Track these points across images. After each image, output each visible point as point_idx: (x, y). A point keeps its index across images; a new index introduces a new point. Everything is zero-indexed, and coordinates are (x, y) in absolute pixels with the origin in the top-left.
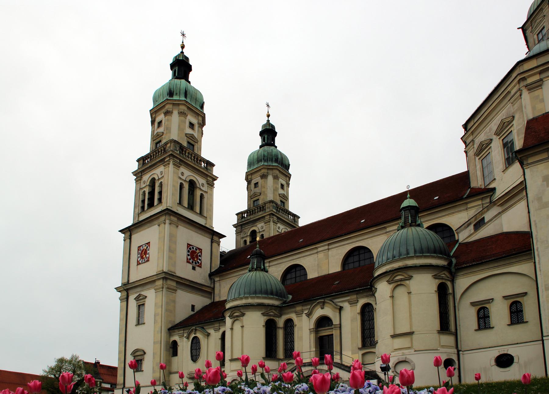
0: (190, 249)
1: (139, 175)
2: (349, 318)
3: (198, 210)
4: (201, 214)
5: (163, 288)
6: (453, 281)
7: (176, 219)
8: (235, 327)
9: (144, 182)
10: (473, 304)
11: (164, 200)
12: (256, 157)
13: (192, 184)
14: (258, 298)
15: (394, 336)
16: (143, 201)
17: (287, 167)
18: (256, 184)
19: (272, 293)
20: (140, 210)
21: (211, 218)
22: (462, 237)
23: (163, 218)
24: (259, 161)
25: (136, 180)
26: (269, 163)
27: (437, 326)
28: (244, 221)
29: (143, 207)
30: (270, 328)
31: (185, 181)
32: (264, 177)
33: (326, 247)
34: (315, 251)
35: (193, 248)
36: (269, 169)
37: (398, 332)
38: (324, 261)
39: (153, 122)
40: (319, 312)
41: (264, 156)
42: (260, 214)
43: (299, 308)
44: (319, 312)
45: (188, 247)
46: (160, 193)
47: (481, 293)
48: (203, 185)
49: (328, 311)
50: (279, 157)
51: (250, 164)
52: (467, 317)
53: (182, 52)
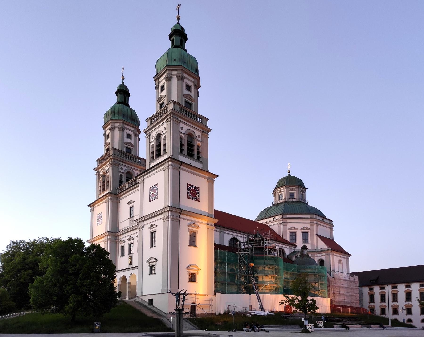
0: (190, 188)
3: (196, 157)
5: (168, 218)
11: (168, 151)
13: (190, 136)
23: (167, 165)
31: (184, 134)
35: (192, 187)
39: (157, 88)
45: (188, 187)
46: (165, 145)
53: (178, 23)
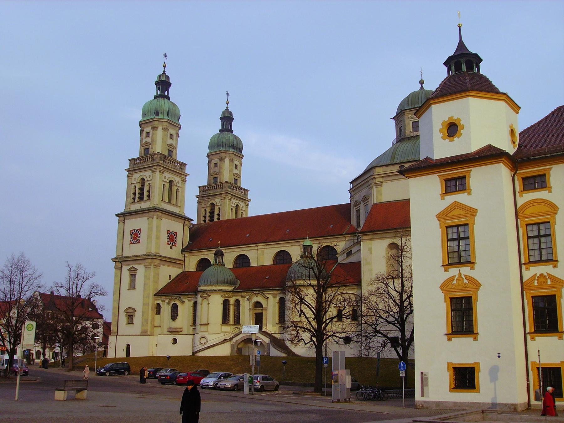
2: (271, 304)
4: (176, 205)
7: (160, 214)
8: (204, 304)
9: (135, 179)
12: (216, 141)
14: (219, 286)
17: (240, 150)
18: (216, 164)
19: (227, 283)
20: (132, 201)
21: (183, 207)
22: (341, 259)
24: (219, 145)
25: (129, 176)
26: (226, 146)
28: (205, 194)
30: (226, 304)
32: (221, 159)
33: (264, 247)
34: (256, 248)
38: (262, 256)
40: (255, 299)
42: (218, 191)
43: (243, 294)
44: (255, 299)
46: (149, 191)
48: (178, 183)
49: (260, 299)
50: (235, 143)
51: (211, 146)
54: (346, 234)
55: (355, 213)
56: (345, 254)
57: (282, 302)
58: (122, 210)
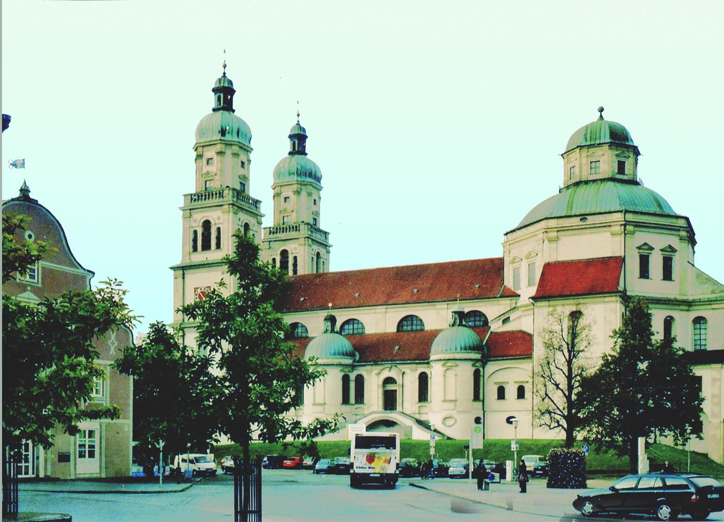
1: (189, 211)
6: (484, 368)
10: (496, 383)
15: (445, 401)
16: (195, 240)
17: (318, 179)
20: (191, 250)
27: (472, 397)
29: (195, 249)
36: (302, 184)
37: (448, 398)
41: (297, 169)
46: (218, 238)
47: (501, 378)
50: (313, 171)
52: (491, 392)
54: (499, 297)
55: (511, 272)
56: (501, 321)
57: (423, 380)
58: (178, 262)
